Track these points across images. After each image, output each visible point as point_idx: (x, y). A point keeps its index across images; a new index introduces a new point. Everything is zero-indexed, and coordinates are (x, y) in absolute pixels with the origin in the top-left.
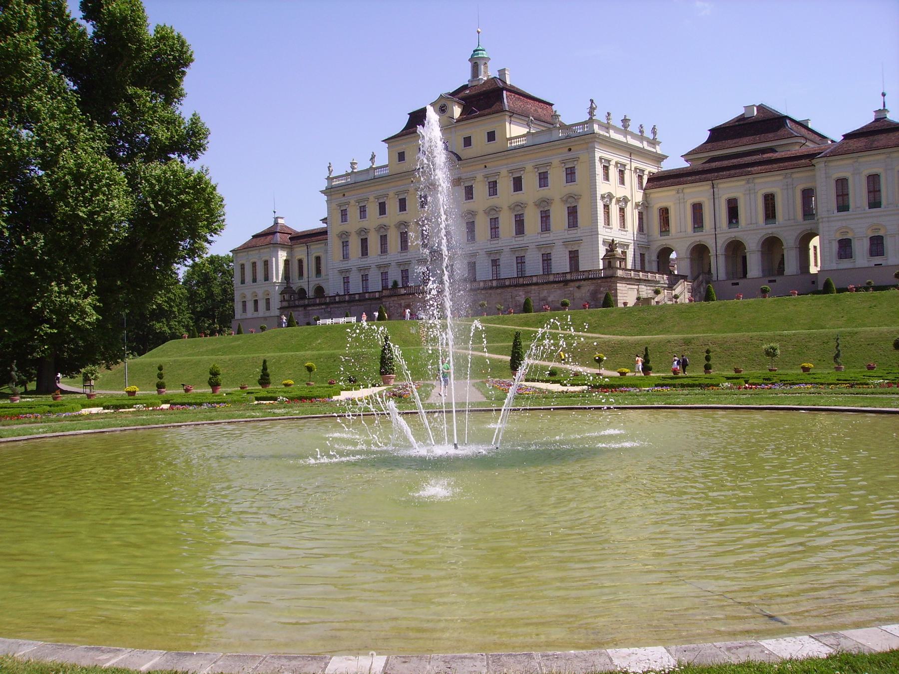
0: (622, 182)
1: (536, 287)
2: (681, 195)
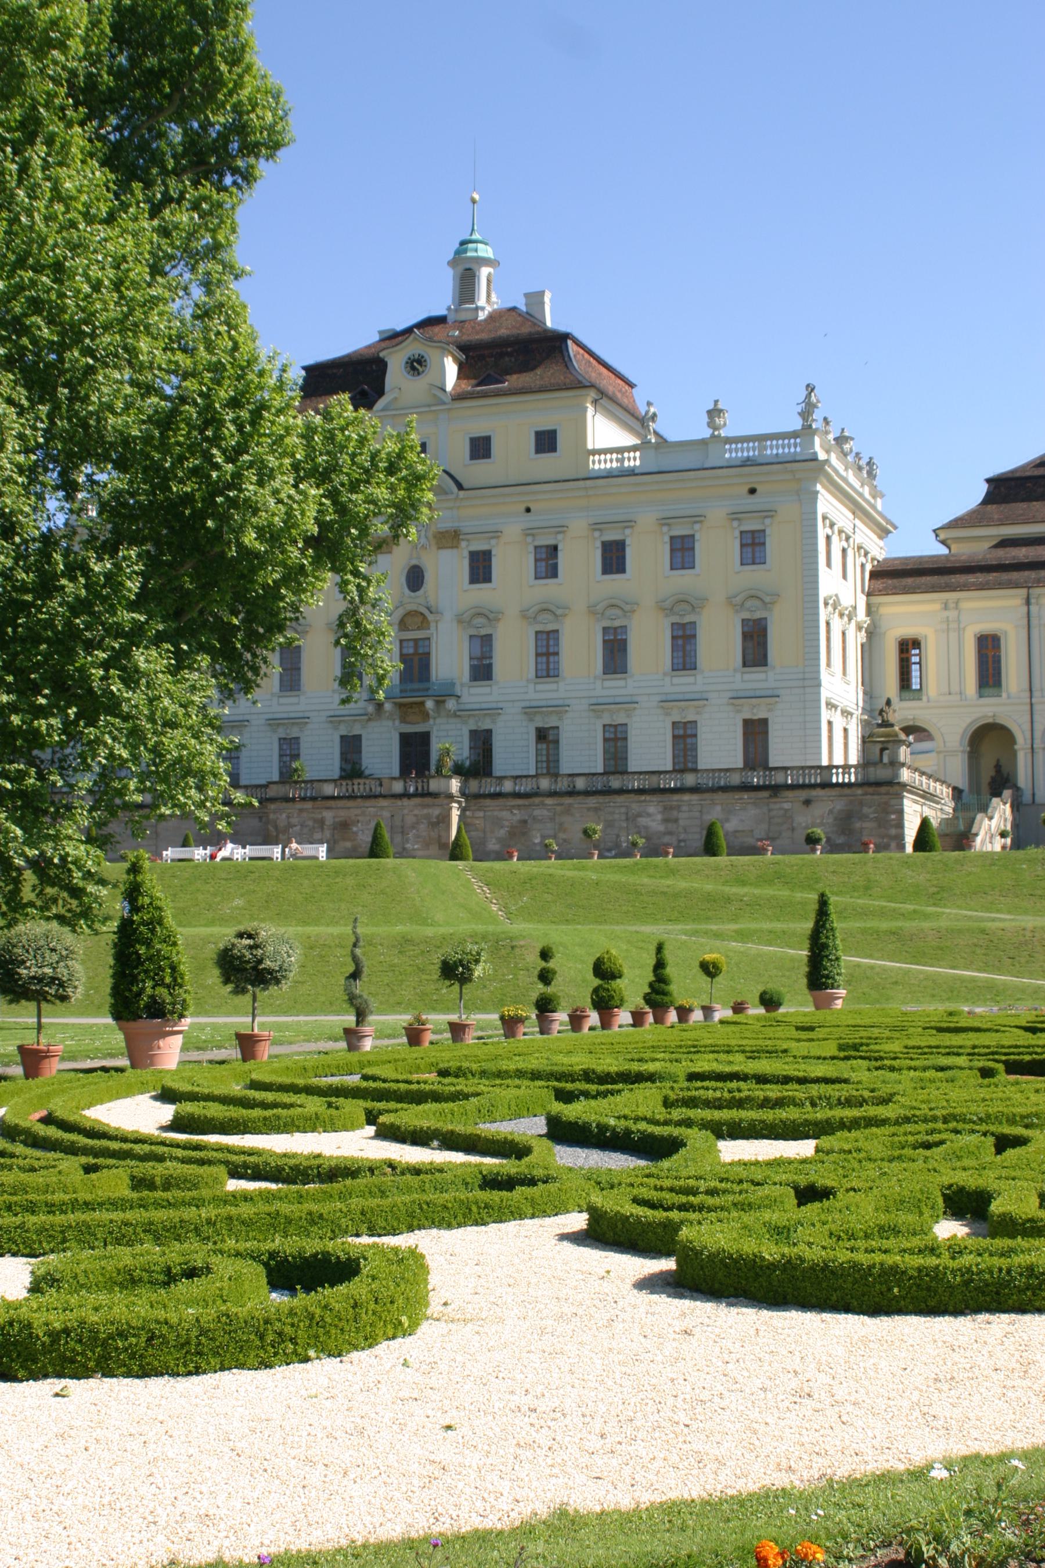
0: (845, 577)
1: (695, 797)
2: (952, 614)
